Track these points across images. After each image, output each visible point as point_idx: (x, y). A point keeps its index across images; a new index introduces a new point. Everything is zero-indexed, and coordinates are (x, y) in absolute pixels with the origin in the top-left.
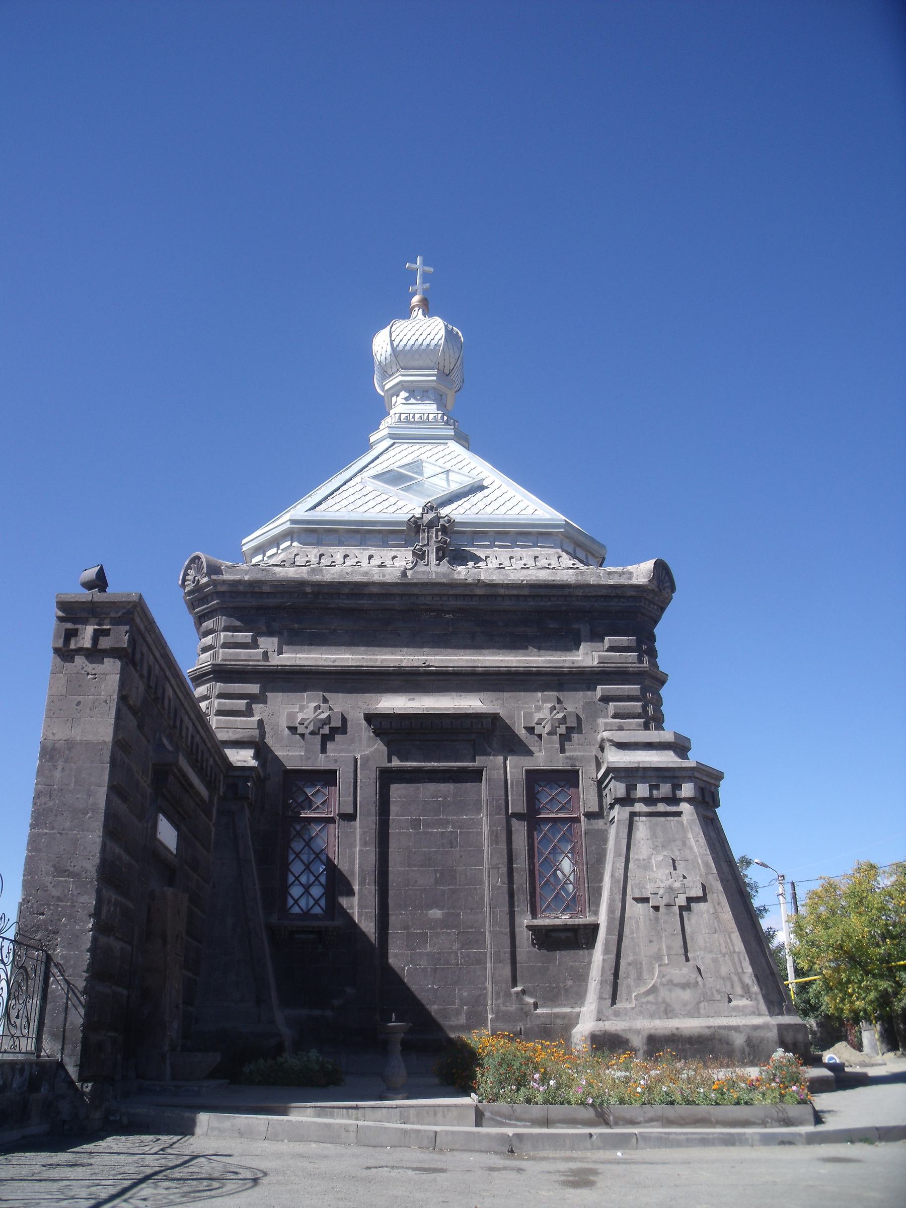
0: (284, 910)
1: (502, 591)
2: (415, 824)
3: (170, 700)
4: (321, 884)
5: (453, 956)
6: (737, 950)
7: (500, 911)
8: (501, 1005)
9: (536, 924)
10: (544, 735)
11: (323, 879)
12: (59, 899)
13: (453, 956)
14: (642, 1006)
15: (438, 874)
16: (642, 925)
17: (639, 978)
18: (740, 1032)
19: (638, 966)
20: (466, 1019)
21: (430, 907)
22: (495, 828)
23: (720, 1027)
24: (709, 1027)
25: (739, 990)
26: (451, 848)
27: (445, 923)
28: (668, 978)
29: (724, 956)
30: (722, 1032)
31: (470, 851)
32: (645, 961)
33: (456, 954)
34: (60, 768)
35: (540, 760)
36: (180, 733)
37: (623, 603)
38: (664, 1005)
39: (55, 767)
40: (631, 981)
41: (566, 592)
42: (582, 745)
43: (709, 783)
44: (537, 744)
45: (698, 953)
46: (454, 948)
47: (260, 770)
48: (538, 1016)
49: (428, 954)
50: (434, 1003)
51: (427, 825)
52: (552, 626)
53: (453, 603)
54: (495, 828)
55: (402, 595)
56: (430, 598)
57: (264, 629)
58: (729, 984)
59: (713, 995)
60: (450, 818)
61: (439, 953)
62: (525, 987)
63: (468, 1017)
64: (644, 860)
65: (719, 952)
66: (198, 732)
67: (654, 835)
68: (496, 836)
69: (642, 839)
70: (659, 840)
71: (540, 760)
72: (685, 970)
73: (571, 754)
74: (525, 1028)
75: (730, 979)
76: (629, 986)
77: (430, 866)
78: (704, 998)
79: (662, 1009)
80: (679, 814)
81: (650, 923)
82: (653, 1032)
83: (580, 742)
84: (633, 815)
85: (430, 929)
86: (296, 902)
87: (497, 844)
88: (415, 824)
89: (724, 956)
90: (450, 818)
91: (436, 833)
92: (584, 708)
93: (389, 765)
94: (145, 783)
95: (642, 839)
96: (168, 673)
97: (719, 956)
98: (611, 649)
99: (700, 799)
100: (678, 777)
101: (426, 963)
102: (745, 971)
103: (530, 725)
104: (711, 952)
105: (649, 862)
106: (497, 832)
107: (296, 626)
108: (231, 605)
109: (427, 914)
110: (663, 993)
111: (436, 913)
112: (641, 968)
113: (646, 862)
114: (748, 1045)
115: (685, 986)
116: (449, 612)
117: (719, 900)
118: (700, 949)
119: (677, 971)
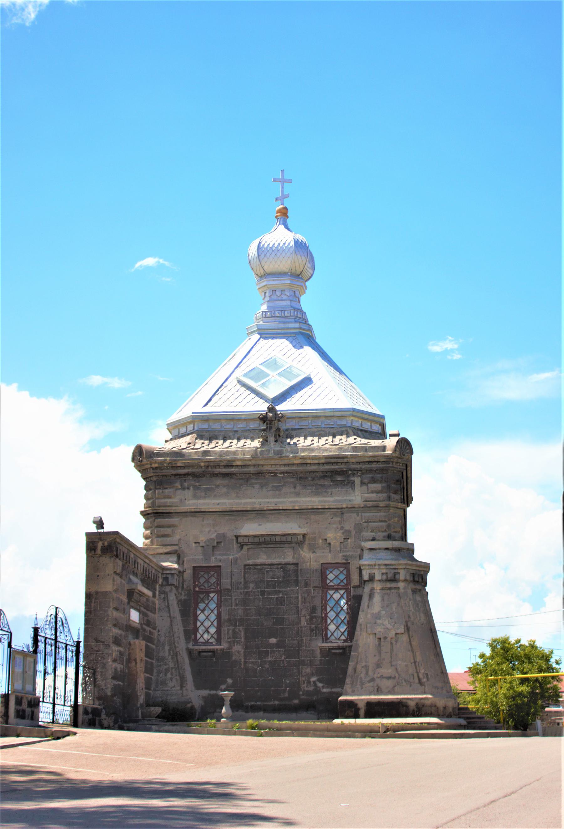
0: (196, 641)
1: (309, 461)
2: (263, 593)
3: (132, 558)
4: (214, 626)
6: (418, 661)
8: (305, 688)
11: (215, 623)
12: (97, 651)
13: (282, 662)
15: (275, 620)
16: (371, 647)
18: (413, 701)
21: (270, 637)
22: (303, 595)
25: (417, 680)
26: (281, 605)
27: (278, 645)
31: (292, 607)
33: (283, 661)
34: (93, 602)
36: (138, 568)
37: (379, 465)
38: (377, 687)
39: (91, 601)
41: (345, 460)
43: (419, 570)
47: (180, 569)
48: (324, 693)
49: (269, 661)
51: (269, 593)
52: (339, 479)
53: (283, 468)
54: (303, 595)
55: (254, 465)
56: (270, 466)
57: (180, 487)
60: (281, 589)
61: (275, 661)
66: (145, 562)
67: (383, 600)
68: (305, 599)
72: (390, 671)
75: (413, 675)
79: (376, 689)
82: (369, 701)
86: (202, 636)
87: (305, 603)
88: (263, 593)
90: (281, 589)
91: (274, 598)
92: (355, 527)
94: (124, 598)
96: (131, 549)
99: (412, 579)
100: (397, 569)
107: (197, 484)
108: (161, 474)
109: (269, 641)
110: (378, 681)
111: (273, 641)
112: (368, 669)
114: (417, 708)
115: (389, 678)
116: (280, 473)
119: (386, 671)
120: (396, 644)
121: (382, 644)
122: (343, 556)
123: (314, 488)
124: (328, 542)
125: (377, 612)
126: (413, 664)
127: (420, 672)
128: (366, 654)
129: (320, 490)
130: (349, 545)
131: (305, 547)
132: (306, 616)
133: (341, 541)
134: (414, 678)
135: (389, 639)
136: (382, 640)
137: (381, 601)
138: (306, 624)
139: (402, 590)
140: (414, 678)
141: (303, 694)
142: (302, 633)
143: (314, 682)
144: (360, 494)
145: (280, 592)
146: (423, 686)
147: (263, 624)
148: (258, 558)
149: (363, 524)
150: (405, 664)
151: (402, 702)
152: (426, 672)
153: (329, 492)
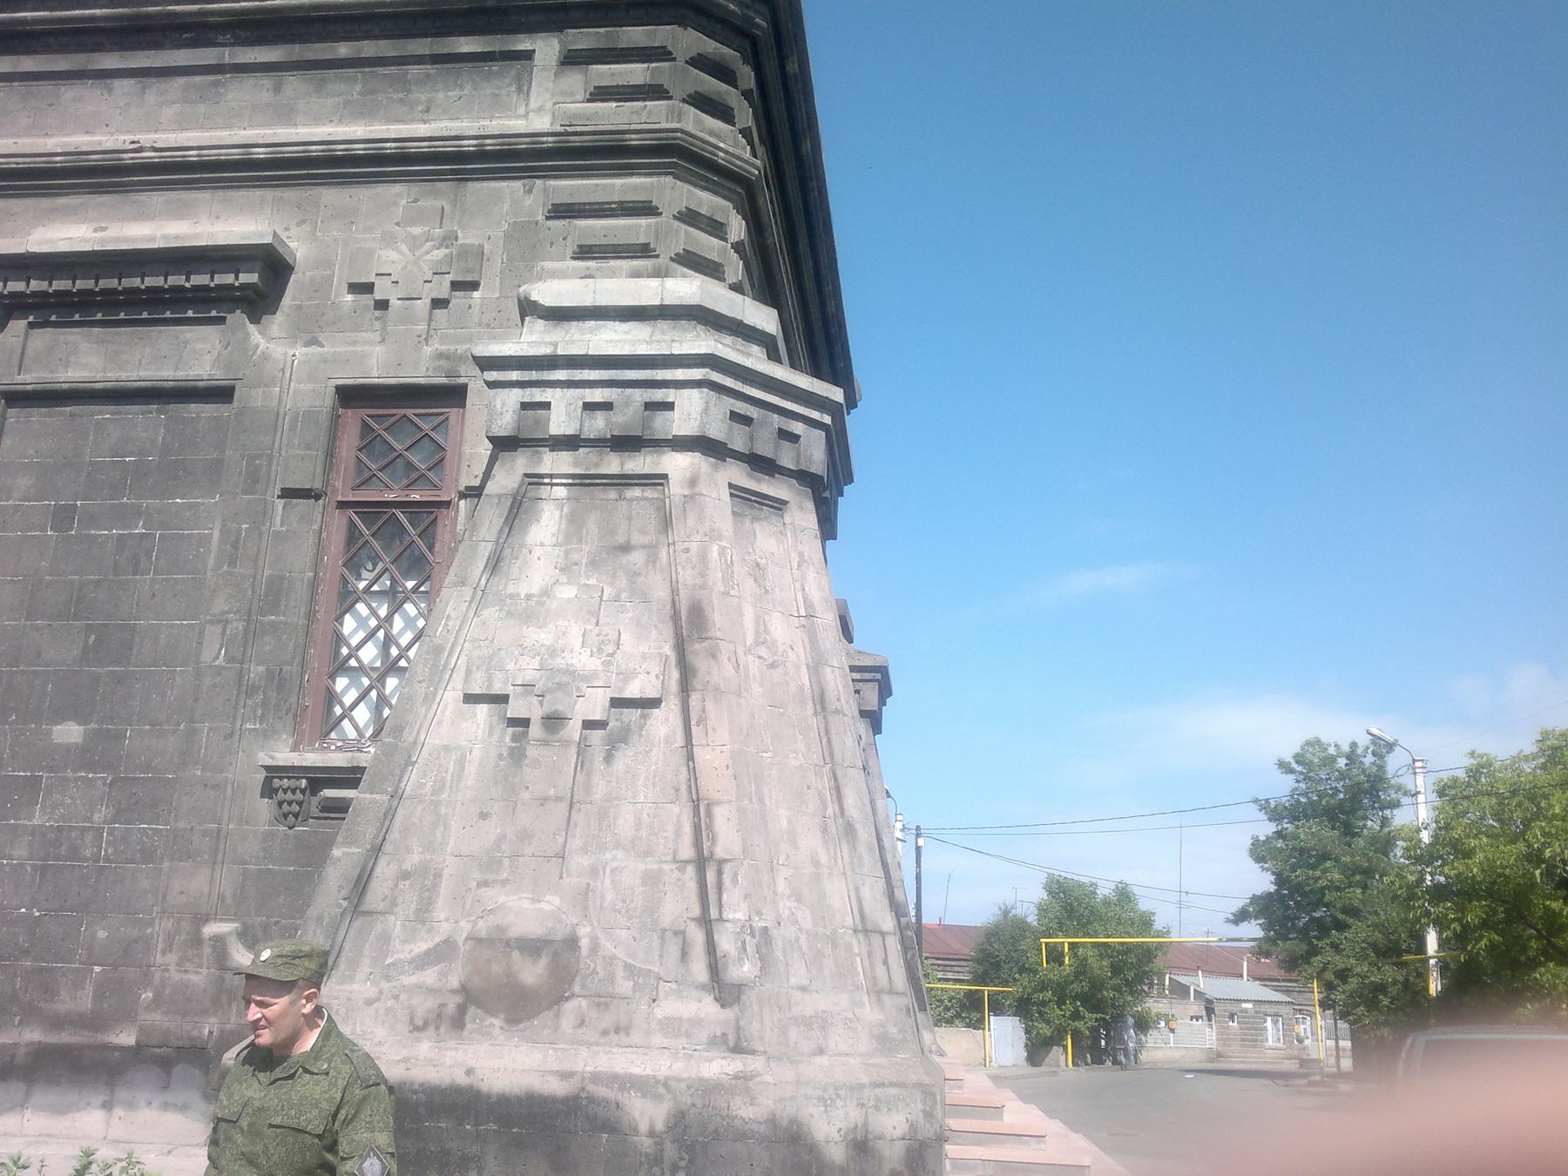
2: (62, 518)
5: (89, 837)
7: (210, 730)
9: (281, 763)
10: (394, 303)
13: (89, 837)
14: (396, 997)
15: (93, 637)
16: (471, 769)
17: (423, 914)
18: (657, 1098)
19: (428, 883)
20: (95, 998)
21: (60, 716)
23: (596, 1078)
24: (565, 1076)
26: (135, 573)
27: (86, 757)
28: (492, 920)
29: (681, 870)
30: (601, 1091)
32: (451, 866)
33: (99, 831)
35: (374, 361)
40: (395, 925)
42: (488, 326)
44: (377, 325)
45: (608, 856)
46: (96, 817)
49: (33, 831)
50: (25, 953)
58: (674, 949)
59: (611, 978)
61: (60, 829)
62: (244, 924)
63: (99, 997)
64: (529, 597)
65: (669, 858)
68: (235, 545)
69: (542, 545)
70: (586, 548)
71: (374, 361)
73: (453, 348)
74: (222, 1032)
75: (680, 933)
76: (386, 938)
77: (76, 617)
78: (583, 986)
80: (657, 480)
81: (498, 765)
83: (485, 320)
84: (534, 480)
85: (51, 769)
87: (232, 563)
89: (681, 870)
92: (508, 237)
93: (20, 378)
95: (542, 545)
97: (666, 867)
98: (601, 94)
101: (24, 853)
102: (725, 917)
103: (363, 280)
104: (647, 854)
105: (541, 604)
106: (239, 533)
109: (49, 733)
111: (70, 733)
112: (435, 886)
113: (532, 603)
117: (704, 711)
118: (617, 845)
119: (526, 904)
120: (608, 759)
121: (532, 752)
122: (441, 356)
123: (358, 87)
124: (378, 295)
125: (535, 590)
126: (690, 871)
127: (721, 919)
128: (438, 803)
129: (380, 97)
130: (476, 310)
131: (277, 322)
132: (227, 622)
133: (435, 295)
134: (684, 955)
135: (574, 730)
136: (535, 730)
137: (567, 540)
138: (220, 661)
139: (676, 488)
140: (684, 955)
141: (158, 1001)
142: (196, 700)
143: (219, 940)
144: (549, 105)
145: (138, 512)
146: (736, 1009)
147: (39, 654)
148: (66, 366)
149: (550, 223)
150: (641, 866)
151: (592, 1100)
152: (758, 924)
153: (418, 102)
